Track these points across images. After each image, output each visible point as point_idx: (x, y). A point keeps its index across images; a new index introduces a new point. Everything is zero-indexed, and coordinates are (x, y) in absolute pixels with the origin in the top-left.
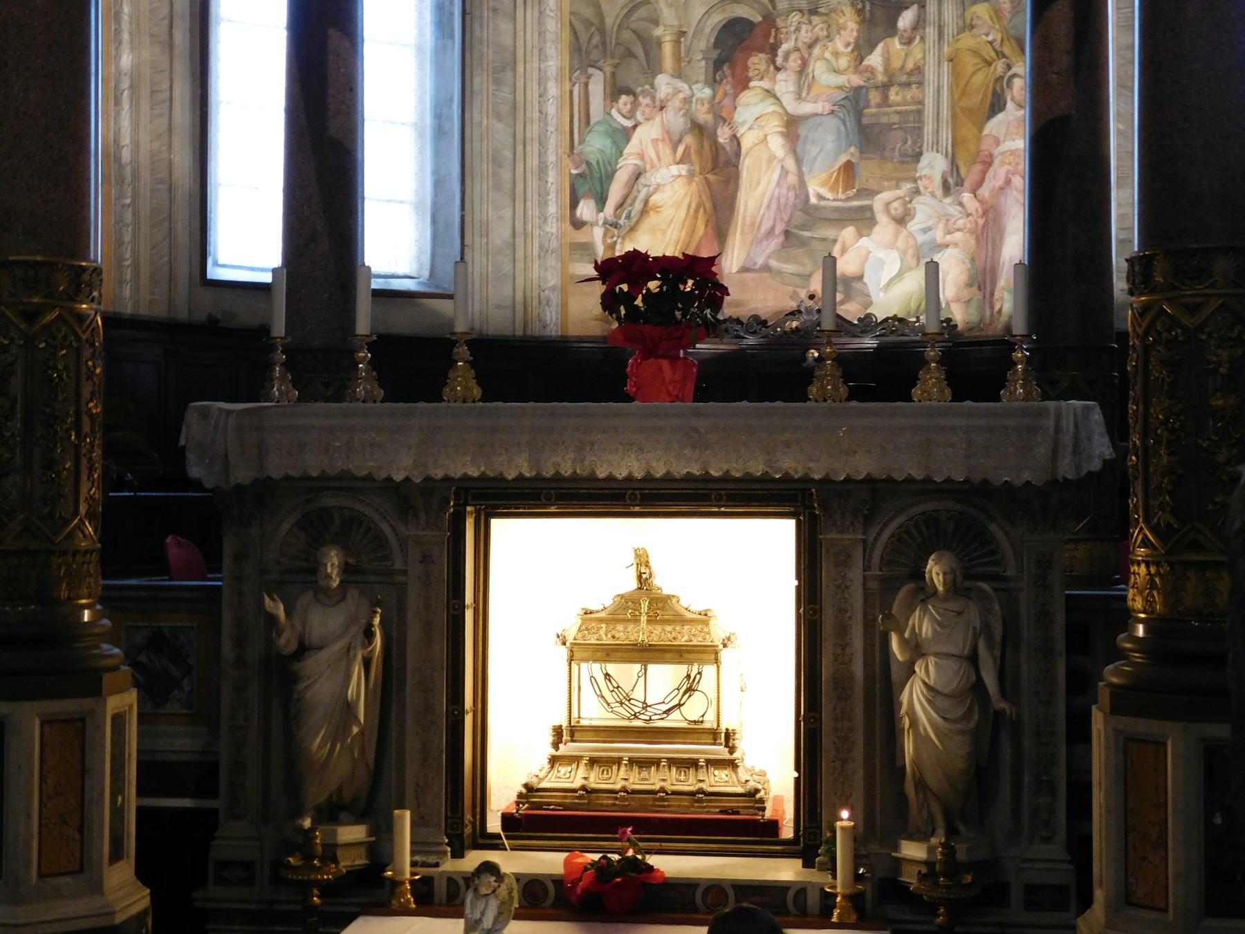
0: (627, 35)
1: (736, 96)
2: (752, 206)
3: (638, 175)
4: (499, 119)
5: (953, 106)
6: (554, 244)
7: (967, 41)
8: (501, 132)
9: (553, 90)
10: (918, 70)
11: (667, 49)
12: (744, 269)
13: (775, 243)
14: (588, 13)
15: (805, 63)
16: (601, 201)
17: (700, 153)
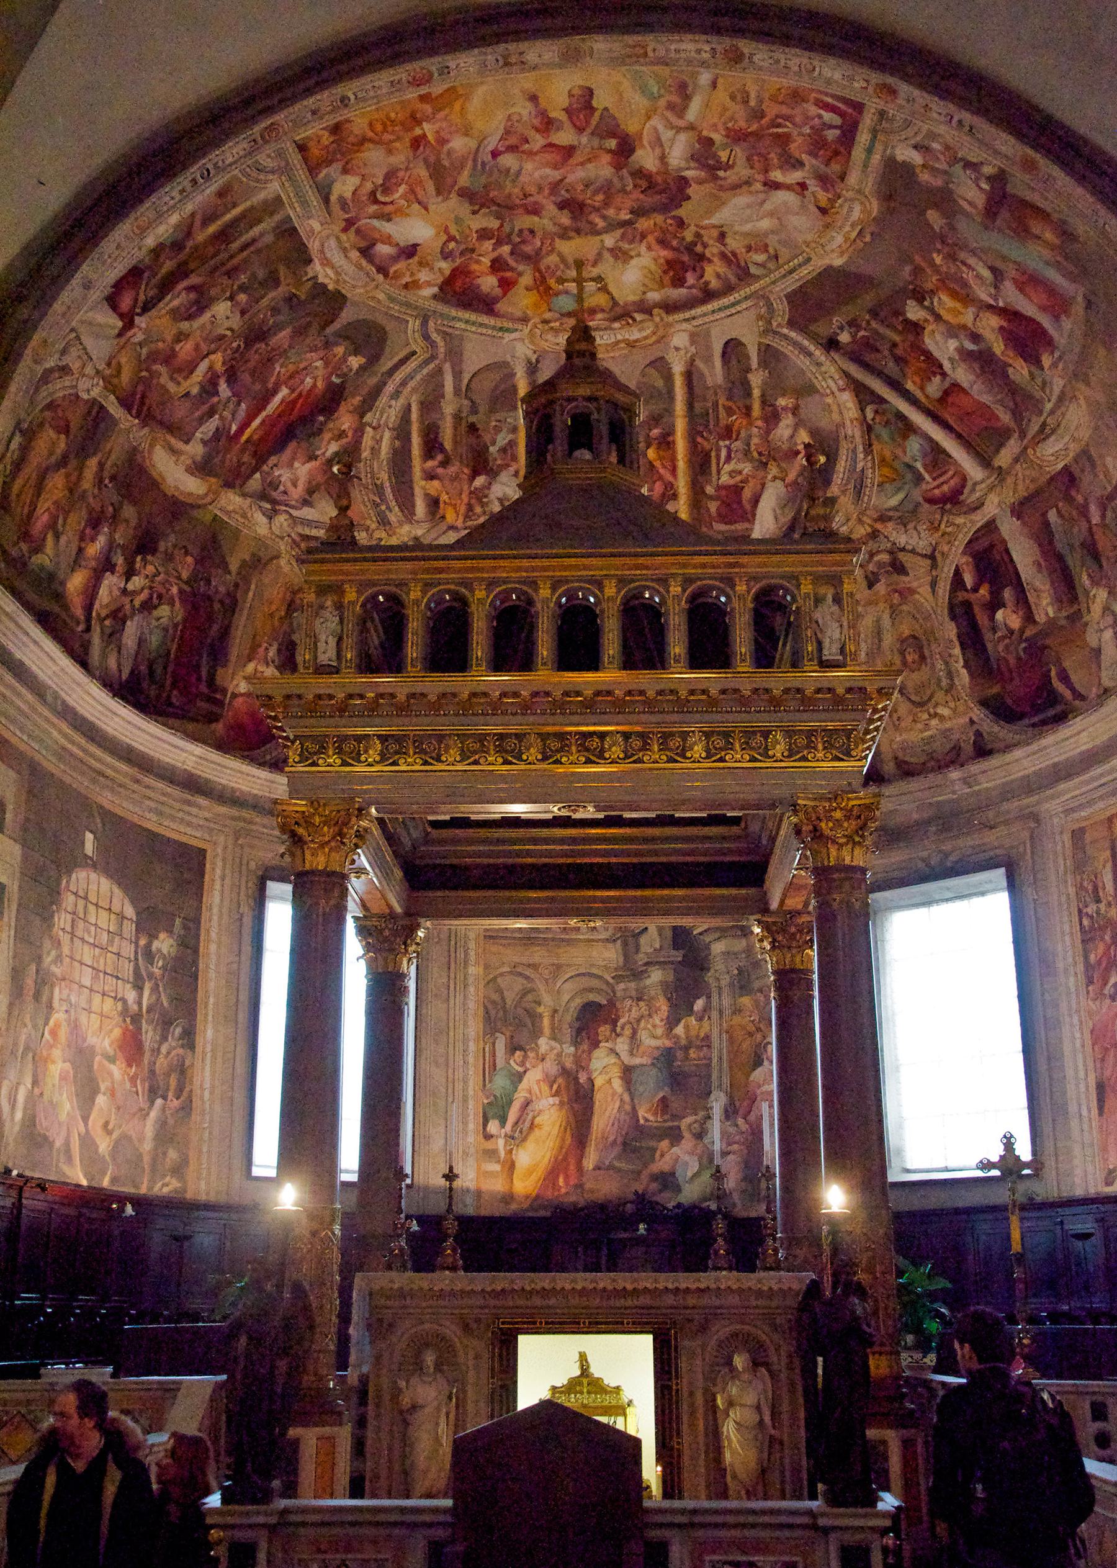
0: (520, 1011)
1: (590, 1052)
2: (601, 1126)
3: (527, 1104)
4: (437, 1065)
5: (730, 1061)
6: (472, 1150)
7: (737, 1019)
8: (438, 1075)
9: (472, 1046)
10: (707, 1037)
11: (546, 1022)
12: (597, 1168)
13: (617, 1150)
14: (495, 997)
15: (634, 1032)
16: (503, 1121)
17: (567, 1088)
